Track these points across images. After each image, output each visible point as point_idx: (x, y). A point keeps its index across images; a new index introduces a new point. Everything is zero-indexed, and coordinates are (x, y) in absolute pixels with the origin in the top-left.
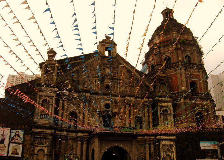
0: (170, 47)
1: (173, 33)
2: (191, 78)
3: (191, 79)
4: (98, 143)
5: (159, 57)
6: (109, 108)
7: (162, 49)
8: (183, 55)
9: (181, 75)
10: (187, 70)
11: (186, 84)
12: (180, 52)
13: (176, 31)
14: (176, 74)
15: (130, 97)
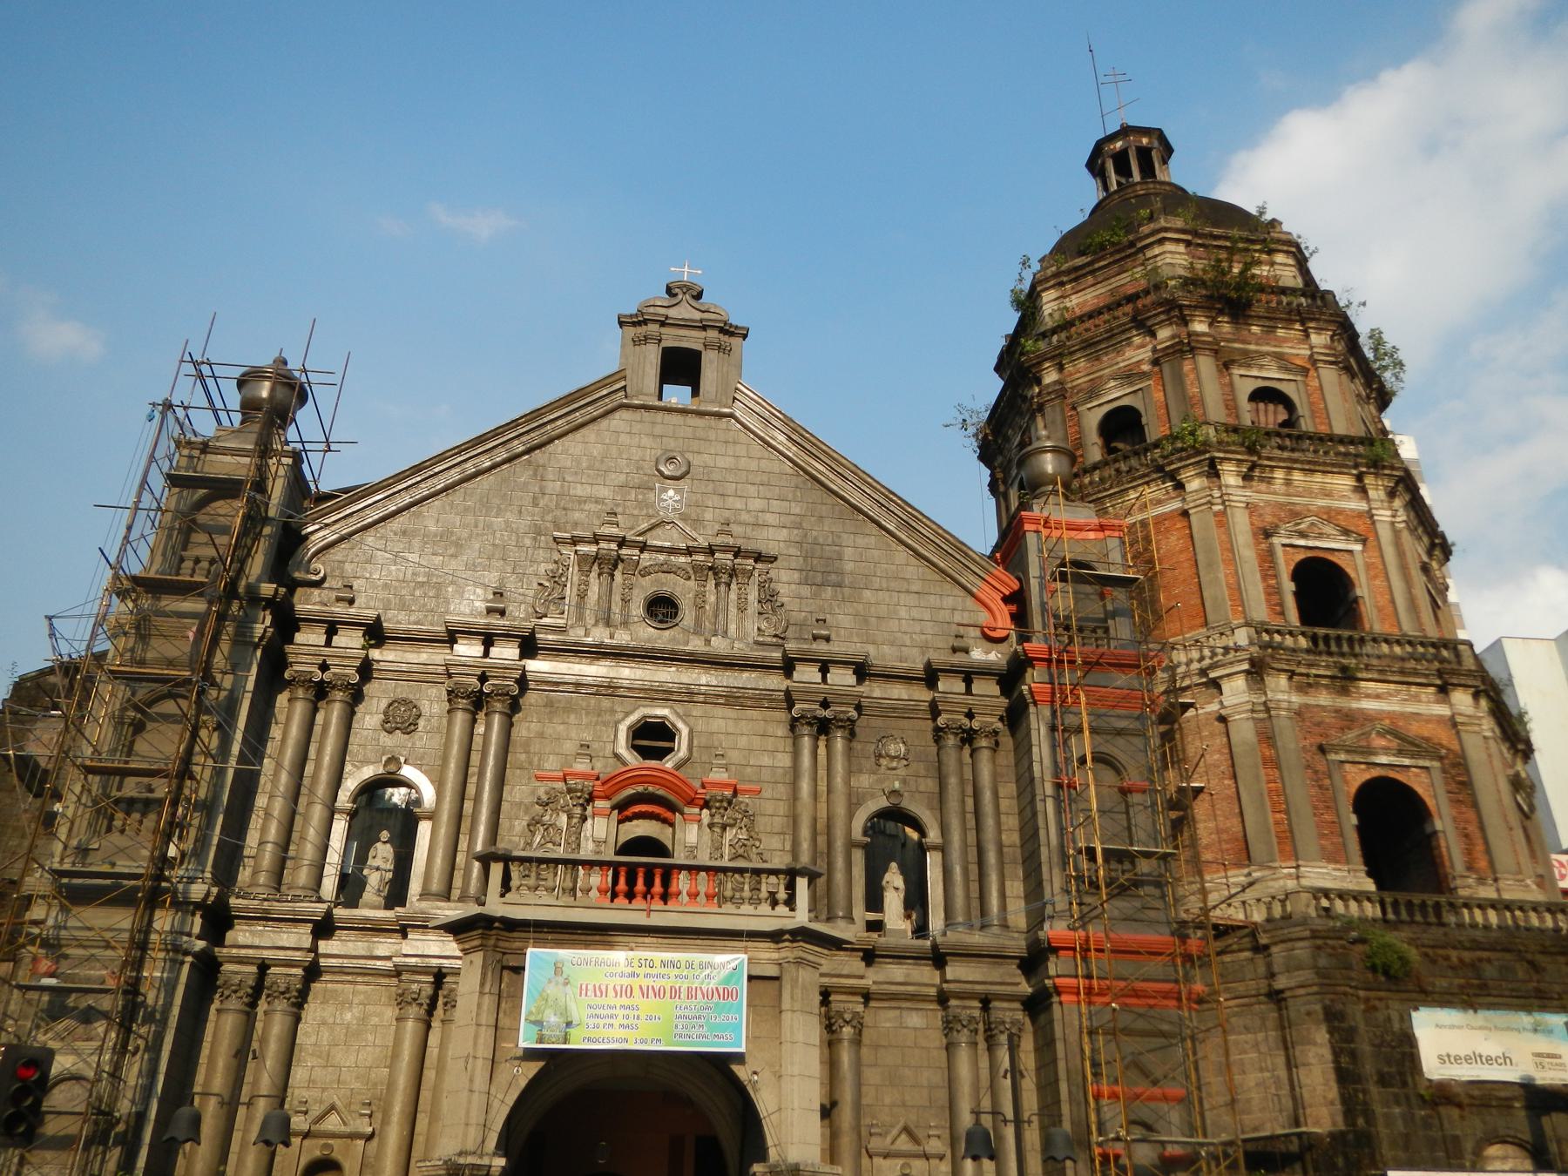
0: (1137, 340)
1: (1157, 250)
2: (1303, 535)
3: (1302, 542)
4: (482, 993)
5: (1059, 419)
6: (672, 750)
7: (1082, 364)
8: (1231, 384)
9: (1222, 519)
10: (1262, 479)
11: (1265, 577)
12: (1206, 364)
13: (1178, 241)
14: (1185, 514)
15: (824, 670)
